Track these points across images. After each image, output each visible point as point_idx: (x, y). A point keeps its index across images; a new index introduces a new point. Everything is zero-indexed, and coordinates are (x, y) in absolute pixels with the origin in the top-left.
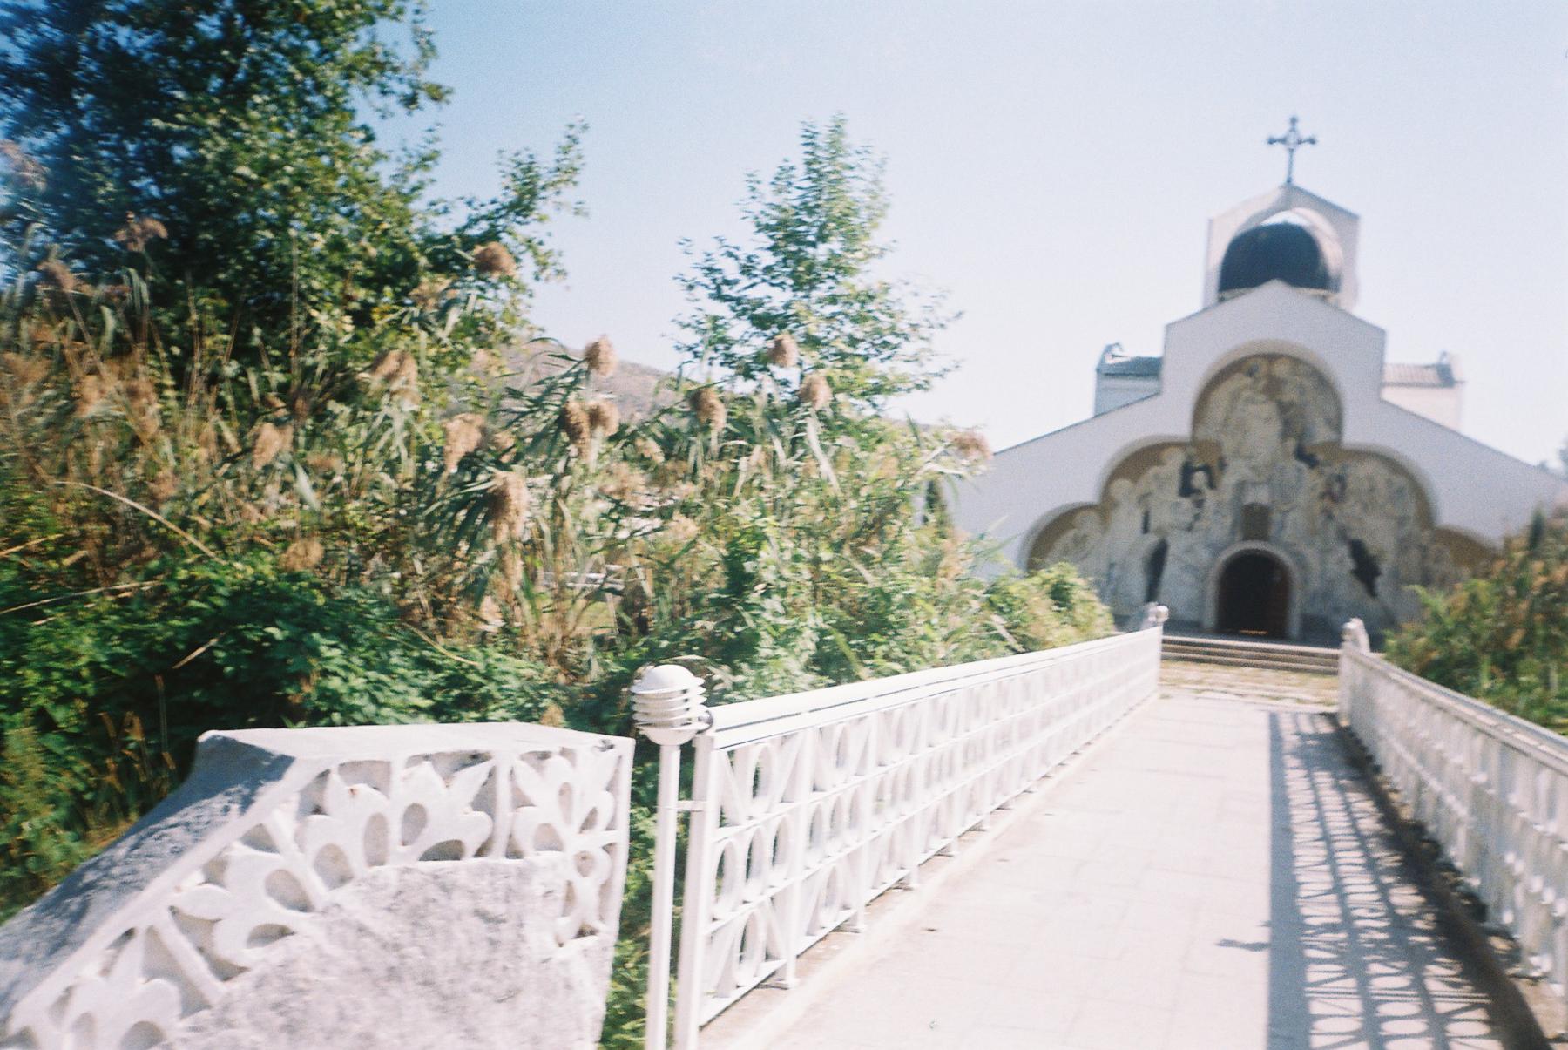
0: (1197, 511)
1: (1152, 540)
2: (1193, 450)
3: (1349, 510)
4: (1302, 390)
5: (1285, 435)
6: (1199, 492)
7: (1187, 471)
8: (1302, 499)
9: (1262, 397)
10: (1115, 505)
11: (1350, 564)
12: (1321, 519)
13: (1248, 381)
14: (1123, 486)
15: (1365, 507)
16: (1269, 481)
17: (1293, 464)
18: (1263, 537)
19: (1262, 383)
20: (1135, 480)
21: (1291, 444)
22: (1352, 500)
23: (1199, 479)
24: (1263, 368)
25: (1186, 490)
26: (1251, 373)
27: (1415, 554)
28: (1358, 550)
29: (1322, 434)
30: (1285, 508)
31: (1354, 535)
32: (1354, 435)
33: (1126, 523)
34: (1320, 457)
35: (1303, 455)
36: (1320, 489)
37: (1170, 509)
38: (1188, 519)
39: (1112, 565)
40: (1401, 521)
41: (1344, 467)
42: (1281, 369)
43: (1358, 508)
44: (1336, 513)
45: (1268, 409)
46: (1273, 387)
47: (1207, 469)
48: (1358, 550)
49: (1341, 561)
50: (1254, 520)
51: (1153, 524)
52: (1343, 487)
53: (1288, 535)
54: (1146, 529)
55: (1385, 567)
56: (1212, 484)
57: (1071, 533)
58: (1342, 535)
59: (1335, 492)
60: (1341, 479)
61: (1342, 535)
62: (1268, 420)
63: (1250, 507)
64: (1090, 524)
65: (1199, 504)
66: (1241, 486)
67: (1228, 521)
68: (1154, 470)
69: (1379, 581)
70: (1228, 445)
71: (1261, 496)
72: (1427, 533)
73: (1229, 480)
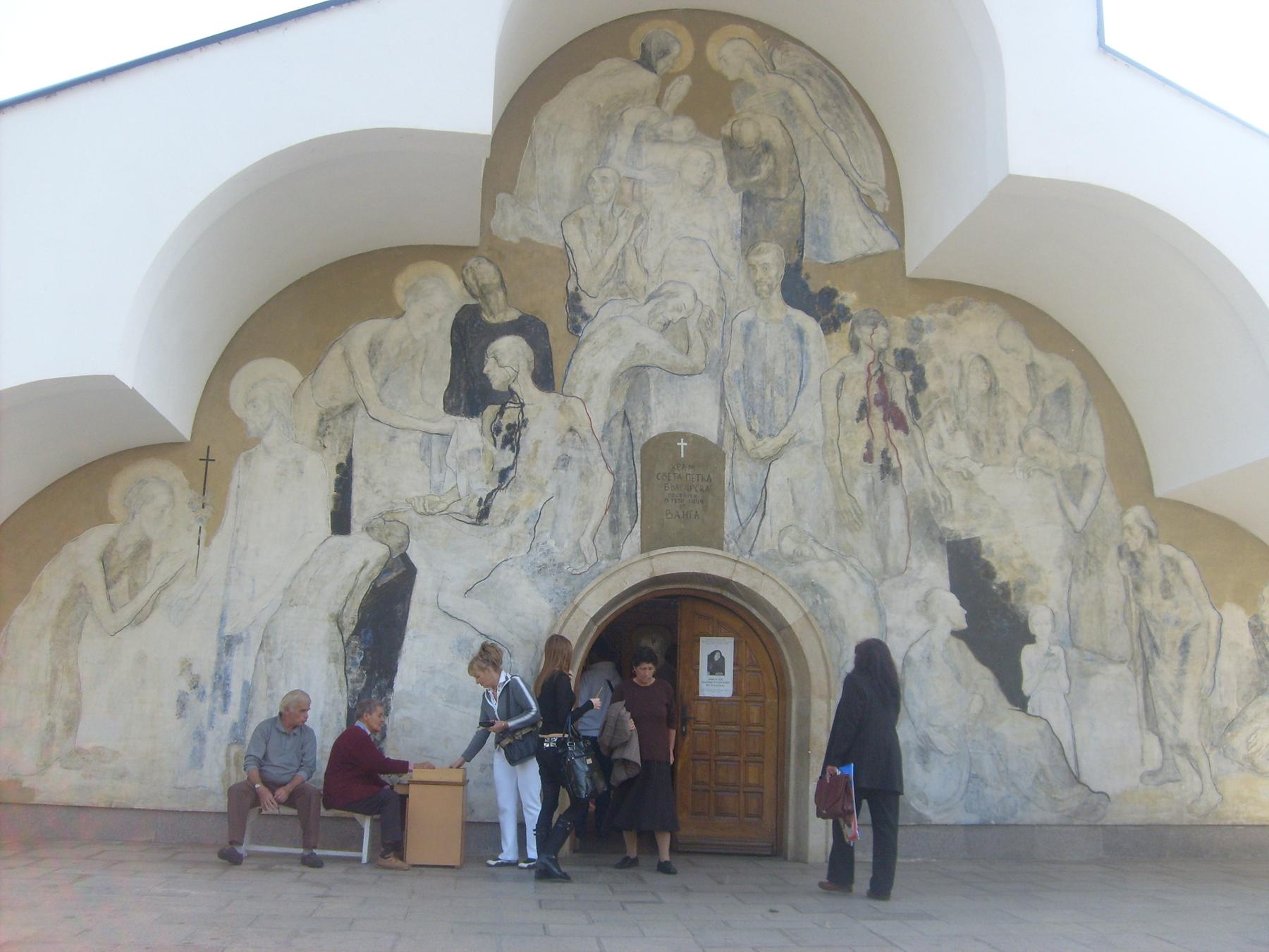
0: (505, 458)
1: (363, 554)
2: (487, 273)
3: (939, 447)
4: (789, 111)
5: (749, 240)
6: (507, 397)
7: (470, 335)
8: (810, 419)
9: (683, 126)
10: (246, 443)
11: (952, 612)
12: (868, 475)
13: (645, 79)
14: (267, 383)
15: (977, 444)
16: (715, 366)
17: (779, 323)
18: (711, 537)
19: (680, 88)
20: (309, 368)
21: (771, 259)
22: (942, 426)
23: (507, 359)
24: (682, 49)
25: (470, 392)
26: (646, 62)
27: (1114, 573)
28: (969, 570)
29: (849, 234)
30: (768, 446)
31: (957, 526)
32: (936, 232)
33: (279, 498)
34: (849, 298)
35: (809, 295)
36: (856, 392)
37: (420, 458)
38: (474, 482)
39: (229, 644)
40: (1074, 481)
41: (917, 330)
42: (731, 55)
43: (961, 445)
44: (904, 460)
45: (702, 160)
46: (710, 103)
47: (530, 328)
48: (969, 570)
49: (925, 605)
50: (676, 482)
51: (364, 503)
52: (919, 383)
53: (774, 530)
54: (341, 522)
55: (1040, 620)
56: (545, 377)
57: (94, 540)
58: (924, 520)
59: (896, 400)
60: (906, 359)
61: (924, 520)
62: (704, 189)
63: (667, 440)
64: (158, 501)
65: (511, 437)
66: (635, 378)
67: (604, 483)
68: (362, 333)
69: (1028, 655)
70: (591, 259)
71: (690, 410)
72: (1137, 513)
73: (596, 363)
